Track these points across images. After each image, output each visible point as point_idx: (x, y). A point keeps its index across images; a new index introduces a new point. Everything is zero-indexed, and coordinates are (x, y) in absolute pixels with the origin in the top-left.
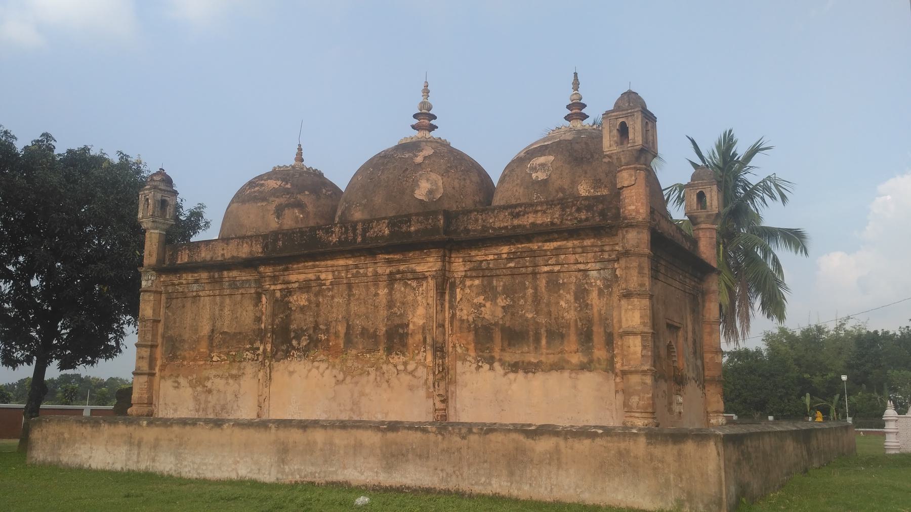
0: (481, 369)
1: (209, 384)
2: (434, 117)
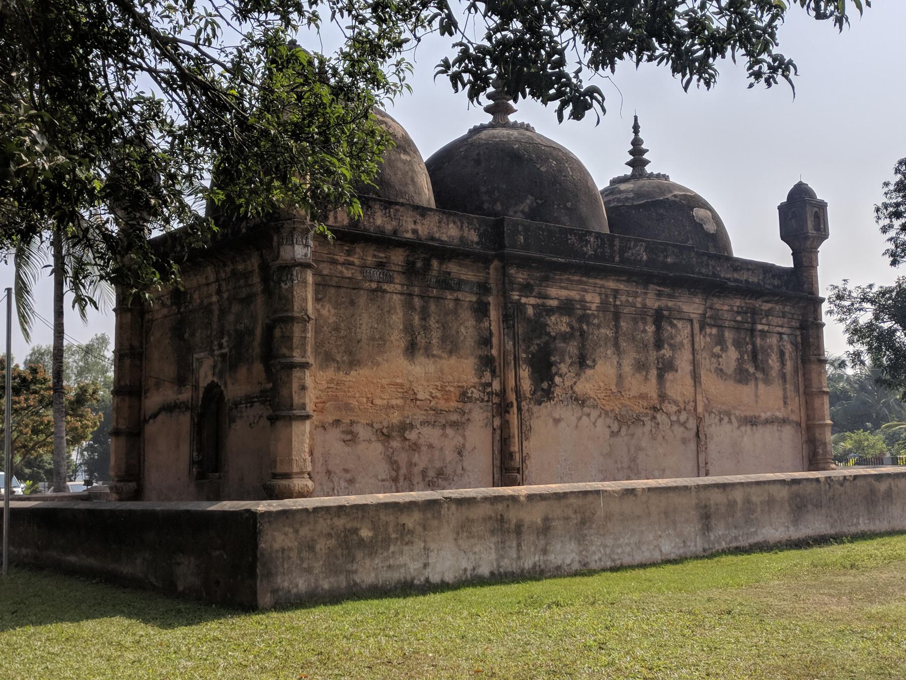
1: (412, 435)
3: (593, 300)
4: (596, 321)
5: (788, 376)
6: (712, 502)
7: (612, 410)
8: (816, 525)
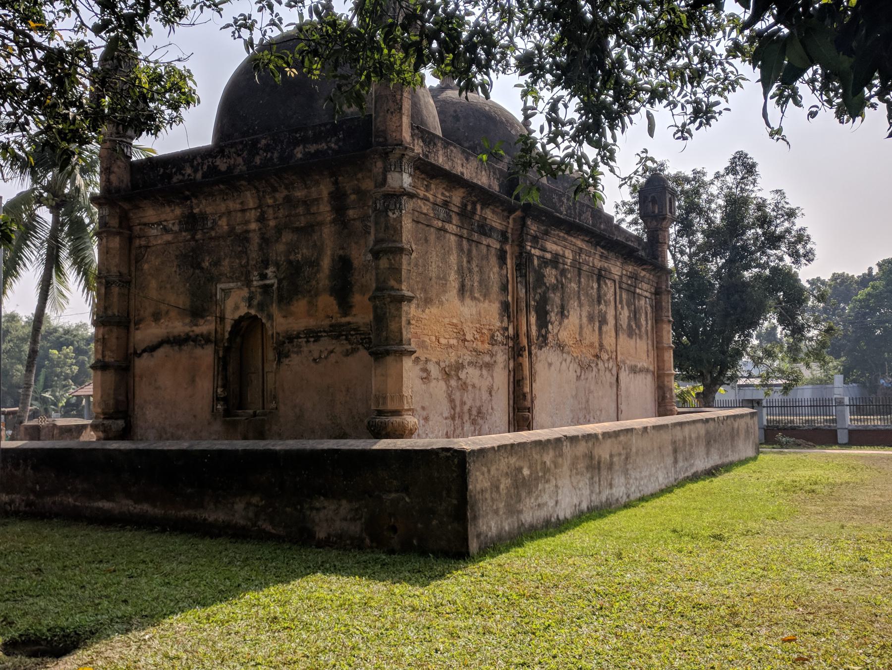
1: (462, 375)
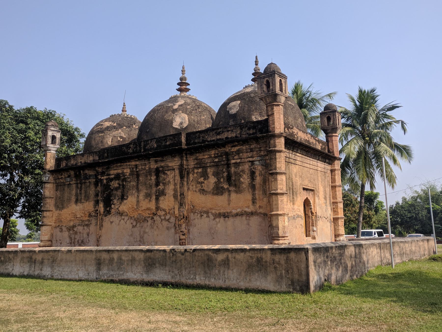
0: (202, 217)
1: (75, 229)
2: (189, 85)
3: (127, 171)
4: (129, 180)
5: (257, 186)
6: (102, 258)
7: (134, 217)
8: (159, 275)
